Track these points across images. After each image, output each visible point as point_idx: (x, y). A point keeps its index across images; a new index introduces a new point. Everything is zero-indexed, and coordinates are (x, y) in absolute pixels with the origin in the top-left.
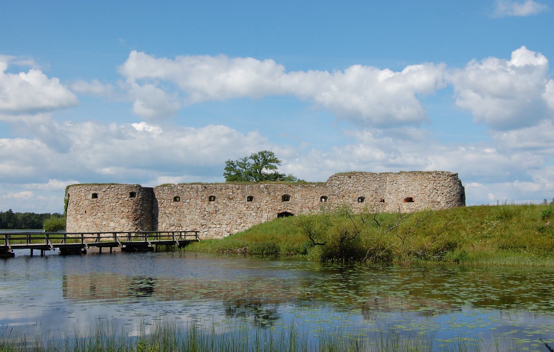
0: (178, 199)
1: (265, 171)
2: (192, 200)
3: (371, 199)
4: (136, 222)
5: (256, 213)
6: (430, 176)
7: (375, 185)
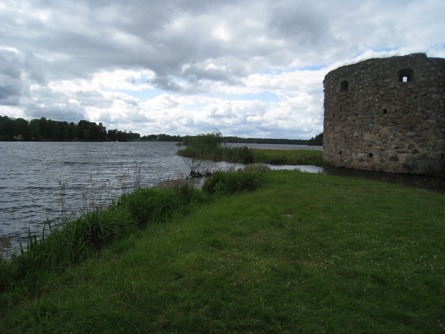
4: (409, 133)
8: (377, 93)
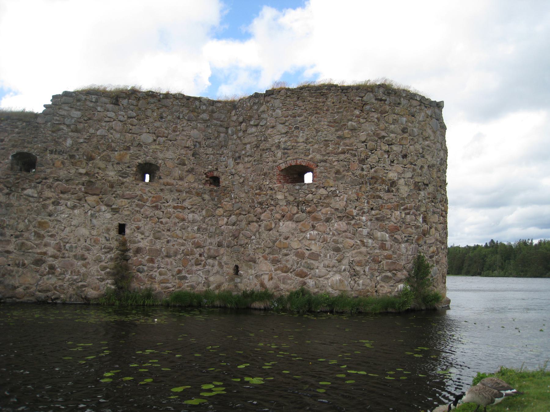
3: (177, 172)
6: (369, 97)
7: (194, 133)
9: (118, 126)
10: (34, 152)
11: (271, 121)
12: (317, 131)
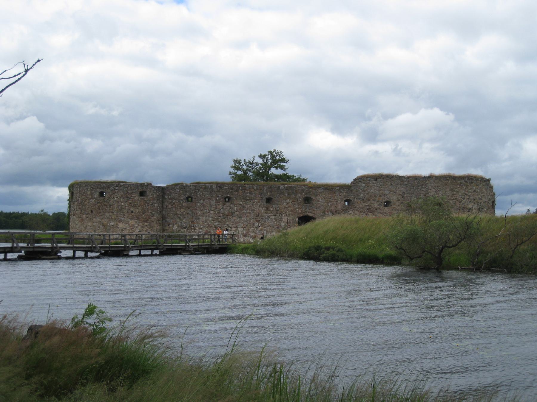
0: (190, 199)
1: (273, 171)
2: (206, 200)
3: (397, 204)
4: (146, 224)
5: (275, 216)
6: (463, 181)
8: (126, 202)
9: (377, 188)
10: (351, 199)
11: (430, 187)
12: (445, 192)
